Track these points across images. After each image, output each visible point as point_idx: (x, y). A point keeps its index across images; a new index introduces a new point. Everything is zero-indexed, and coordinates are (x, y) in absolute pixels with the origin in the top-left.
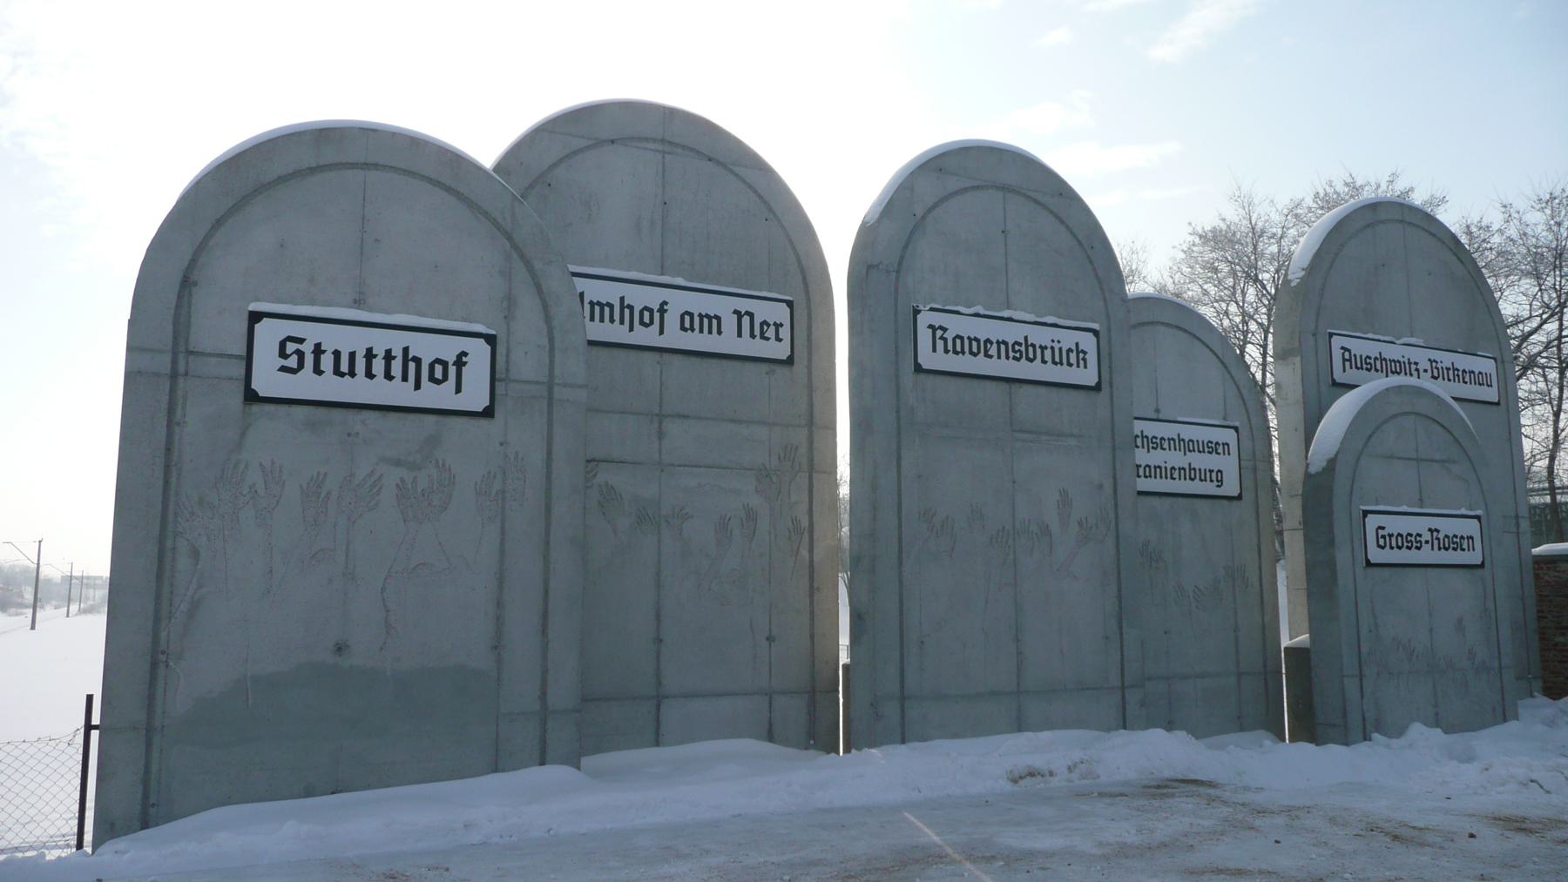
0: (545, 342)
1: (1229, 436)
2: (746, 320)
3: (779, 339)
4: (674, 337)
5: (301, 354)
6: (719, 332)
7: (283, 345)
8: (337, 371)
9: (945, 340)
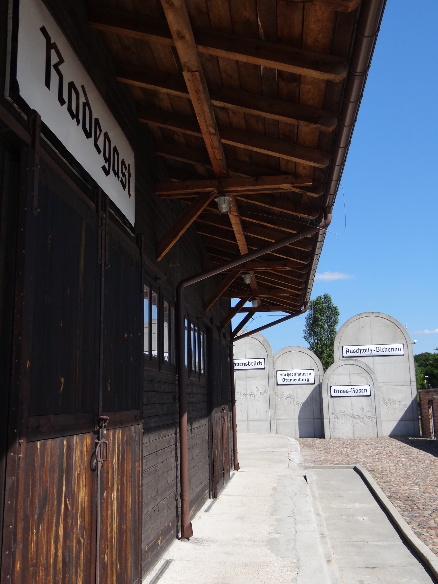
1: (312, 372)
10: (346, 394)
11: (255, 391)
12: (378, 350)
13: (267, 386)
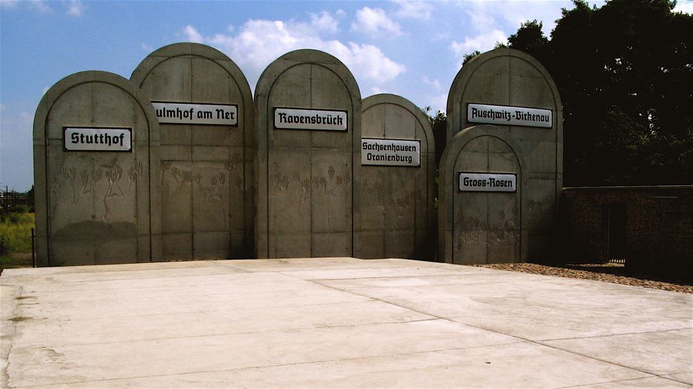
0: (147, 129)
1: (417, 144)
2: (221, 112)
3: (232, 118)
4: (196, 120)
5: (77, 138)
6: (211, 117)
7: (72, 135)
8: (88, 142)
9: (285, 118)
10: (481, 188)
11: (326, 175)
12: (519, 117)
13: (350, 166)
